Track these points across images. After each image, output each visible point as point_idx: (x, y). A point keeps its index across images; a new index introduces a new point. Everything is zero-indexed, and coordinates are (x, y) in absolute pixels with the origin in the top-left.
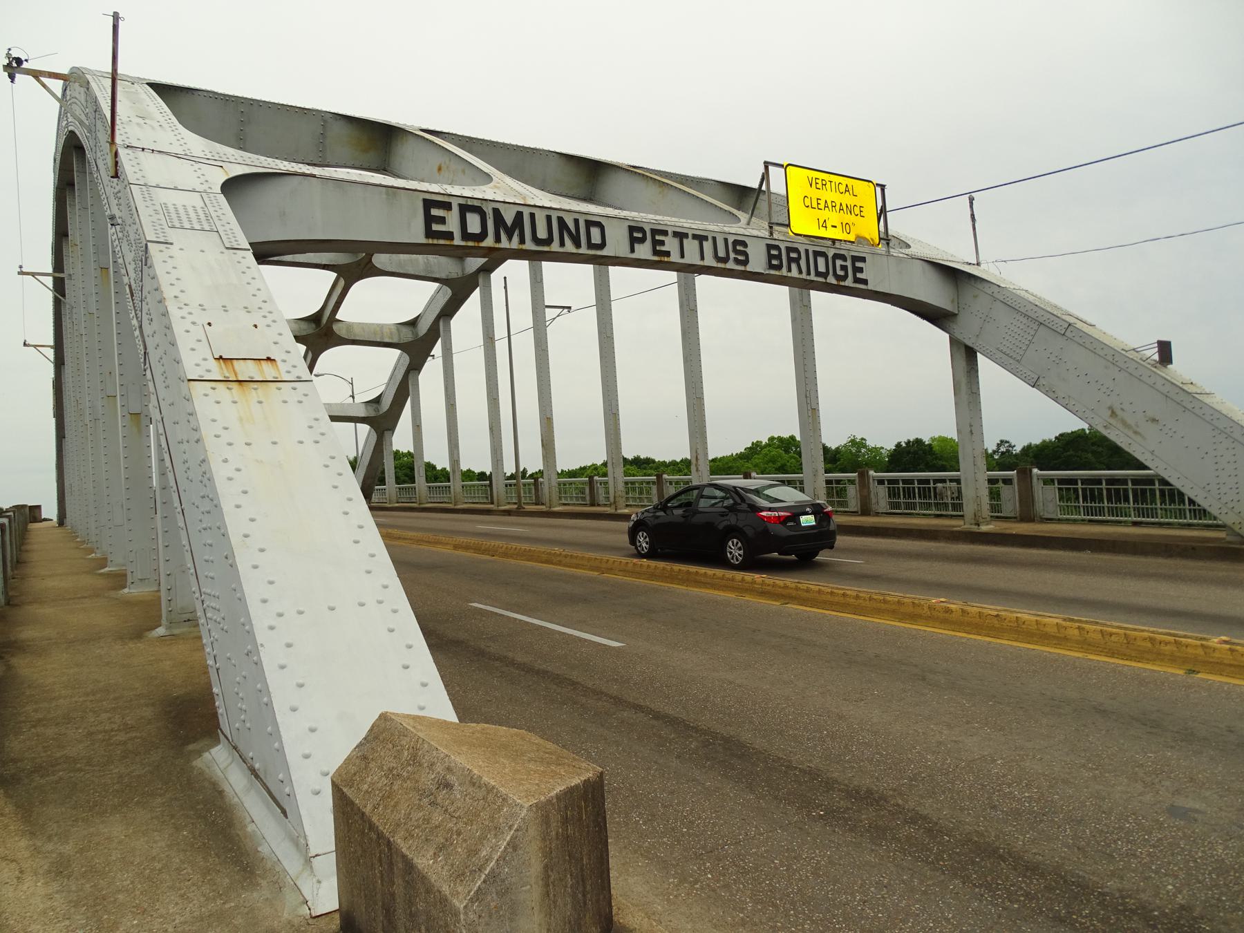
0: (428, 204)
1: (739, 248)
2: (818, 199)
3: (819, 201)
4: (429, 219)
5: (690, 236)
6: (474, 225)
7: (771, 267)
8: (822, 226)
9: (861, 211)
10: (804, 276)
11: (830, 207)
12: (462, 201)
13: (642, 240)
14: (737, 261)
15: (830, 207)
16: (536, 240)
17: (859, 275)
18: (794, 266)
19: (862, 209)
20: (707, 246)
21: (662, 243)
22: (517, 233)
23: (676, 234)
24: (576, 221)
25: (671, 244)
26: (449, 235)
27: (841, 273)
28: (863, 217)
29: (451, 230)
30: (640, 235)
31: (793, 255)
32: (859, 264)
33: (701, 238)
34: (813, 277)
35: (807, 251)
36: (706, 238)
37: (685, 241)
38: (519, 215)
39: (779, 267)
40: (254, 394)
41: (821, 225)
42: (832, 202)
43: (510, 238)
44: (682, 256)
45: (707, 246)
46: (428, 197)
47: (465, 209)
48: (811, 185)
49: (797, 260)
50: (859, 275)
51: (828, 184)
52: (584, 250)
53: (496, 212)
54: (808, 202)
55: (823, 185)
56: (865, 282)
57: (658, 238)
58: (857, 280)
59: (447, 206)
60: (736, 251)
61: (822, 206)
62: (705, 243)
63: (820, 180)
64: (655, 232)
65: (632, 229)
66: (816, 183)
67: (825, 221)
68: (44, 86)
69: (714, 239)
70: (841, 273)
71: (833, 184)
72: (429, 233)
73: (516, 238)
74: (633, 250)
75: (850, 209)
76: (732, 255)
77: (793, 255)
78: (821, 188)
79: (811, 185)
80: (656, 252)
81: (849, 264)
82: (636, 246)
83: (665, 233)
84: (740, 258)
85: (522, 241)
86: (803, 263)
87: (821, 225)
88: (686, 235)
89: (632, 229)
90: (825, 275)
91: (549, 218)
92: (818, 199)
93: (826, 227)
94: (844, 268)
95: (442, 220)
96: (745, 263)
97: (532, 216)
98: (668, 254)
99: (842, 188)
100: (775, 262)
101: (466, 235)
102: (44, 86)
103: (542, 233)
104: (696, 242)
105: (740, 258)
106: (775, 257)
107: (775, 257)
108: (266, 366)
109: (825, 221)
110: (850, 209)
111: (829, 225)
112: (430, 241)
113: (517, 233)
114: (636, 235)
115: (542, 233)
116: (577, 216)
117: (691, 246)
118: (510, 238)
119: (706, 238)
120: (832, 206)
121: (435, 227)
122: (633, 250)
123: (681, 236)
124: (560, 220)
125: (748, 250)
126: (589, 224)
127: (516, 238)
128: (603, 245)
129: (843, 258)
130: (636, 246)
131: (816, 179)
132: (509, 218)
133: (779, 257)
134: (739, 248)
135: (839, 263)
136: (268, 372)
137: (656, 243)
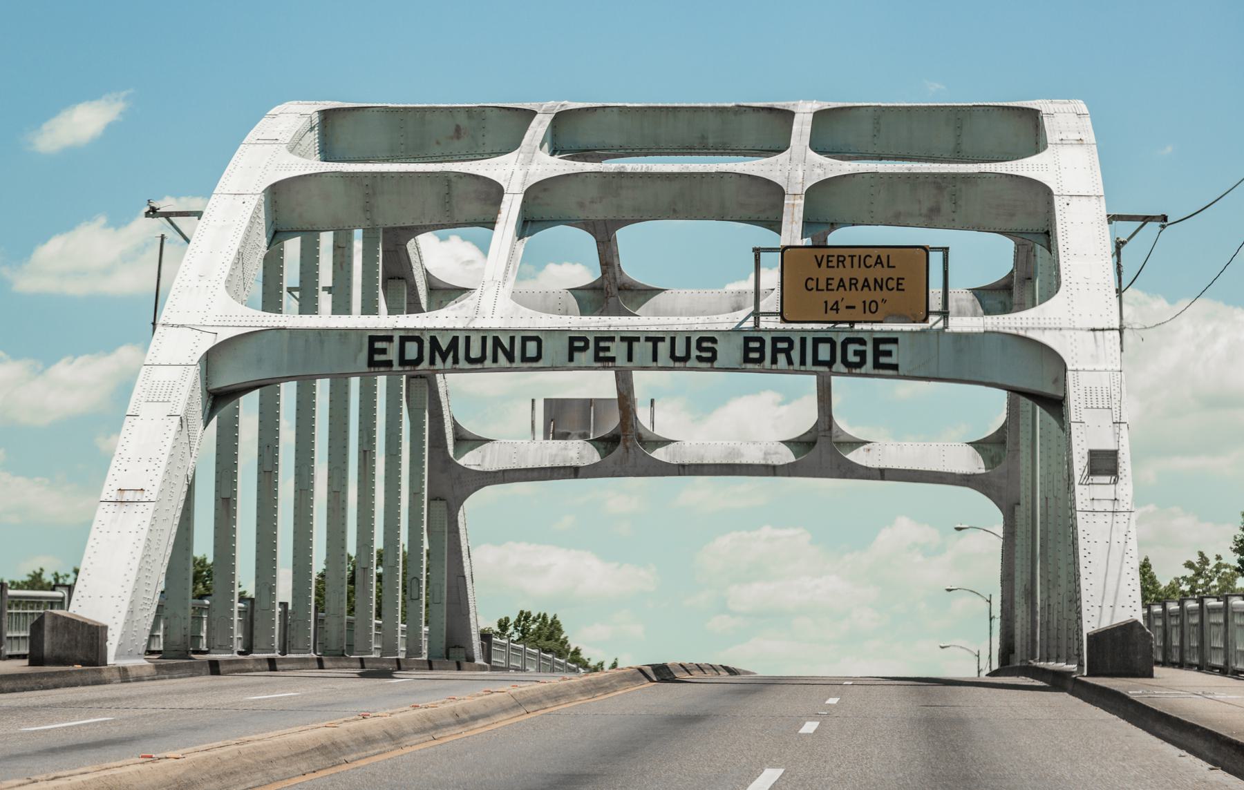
0: (373, 339)
1: (705, 345)
2: (828, 279)
3: (830, 282)
4: (372, 351)
5: (642, 339)
6: (411, 350)
7: (747, 360)
8: (831, 309)
9: (898, 284)
11: (847, 287)
12: (403, 334)
14: (700, 359)
15: (847, 287)
16: (469, 359)
17: (883, 360)
18: (782, 358)
19: (900, 281)
20: (663, 348)
21: (608, 349)
22: (451, 354)
24: (512, 339)
25: (617, 350)
26: (389, 364)
27: (852, 358)
28: (903, 290)
29: (391, 359)
30: (582, 344)
31: (781, 345)
33: (655, 340)
35: (803, 340)
36: (662, 339)
37: (635, 345)
38: (455, 339)
39: (761, 360)
40: (124, 508)
41: (829, 306)
42: (851, 279)
43: (444, 360)
44: (630, 359)
45: (663, 348)
47: (403, 340)
48: (819, 265)
49: (787, 352)
50: (883, 360)
53: (434, 340)
54: (811, 284)
55: (838, 261)
56: (895, 367)
57: (602, 344)
58: (877, 365)
59: (389, 339)
60: (699, 348)
61: (834, 286)
62: (660, 345)
64: (598, 340)
65: (572, 340)
66: (828, 261)
67: (837, 303)
68: (172, 223)
69: (673, 340)
70: (852, 358)
71: (856, 260)
72: (371, 363)
73: (450, 359)
74: (571, 359)
75: (879, 284)
76: (694, 352)
77: (781, 345)
78: (836, 266)
79: (819, 265)
80: (597, 359)
81: (869, 349)
82: (577, 355)
83: (612, 339)
84: (705, 355)
85: (456, 361)
86: (796, 354)
87: (829, 307)
88: (638, 339)
89: (572, 340)
90: (829, 364)
91: (484, 339)
92: (828, 279)
93: (837, 310)
94: (862, 354)
95: (384, 351)
96: (712, 359)
97: (468, 339)
98: (613, 359)
99: (870, 261)
101: (403, 362)
102: (172, 223)
103: (475, 352)
104: (650, 344)
105: (705, 355)
106: (754, 350)
107: (754, 350)
108: (139, 493)
109: (837, 303)
110: (879, 284)
111: (842, 306)
112: (372, 369)
113: (451, 354)
114: (577, 344)
115: (475, 352)
117: (642, 350)
118: (444, 360)
119: (662, 339)
120: (851, 284)
121: (377, 358)
122: (571, 359)
123: (630, 340)
124: (496, 340)
126: (525, 340)
127: (450, 359)
128: (538, 358)
129: (862, 342)
130: (577, 355)
131: (828, 256)
132: (444, 343)
133: (761, 350)
134: (705, 345)
135: (852, 348)
136: (138, 496)
137: (598, 349)
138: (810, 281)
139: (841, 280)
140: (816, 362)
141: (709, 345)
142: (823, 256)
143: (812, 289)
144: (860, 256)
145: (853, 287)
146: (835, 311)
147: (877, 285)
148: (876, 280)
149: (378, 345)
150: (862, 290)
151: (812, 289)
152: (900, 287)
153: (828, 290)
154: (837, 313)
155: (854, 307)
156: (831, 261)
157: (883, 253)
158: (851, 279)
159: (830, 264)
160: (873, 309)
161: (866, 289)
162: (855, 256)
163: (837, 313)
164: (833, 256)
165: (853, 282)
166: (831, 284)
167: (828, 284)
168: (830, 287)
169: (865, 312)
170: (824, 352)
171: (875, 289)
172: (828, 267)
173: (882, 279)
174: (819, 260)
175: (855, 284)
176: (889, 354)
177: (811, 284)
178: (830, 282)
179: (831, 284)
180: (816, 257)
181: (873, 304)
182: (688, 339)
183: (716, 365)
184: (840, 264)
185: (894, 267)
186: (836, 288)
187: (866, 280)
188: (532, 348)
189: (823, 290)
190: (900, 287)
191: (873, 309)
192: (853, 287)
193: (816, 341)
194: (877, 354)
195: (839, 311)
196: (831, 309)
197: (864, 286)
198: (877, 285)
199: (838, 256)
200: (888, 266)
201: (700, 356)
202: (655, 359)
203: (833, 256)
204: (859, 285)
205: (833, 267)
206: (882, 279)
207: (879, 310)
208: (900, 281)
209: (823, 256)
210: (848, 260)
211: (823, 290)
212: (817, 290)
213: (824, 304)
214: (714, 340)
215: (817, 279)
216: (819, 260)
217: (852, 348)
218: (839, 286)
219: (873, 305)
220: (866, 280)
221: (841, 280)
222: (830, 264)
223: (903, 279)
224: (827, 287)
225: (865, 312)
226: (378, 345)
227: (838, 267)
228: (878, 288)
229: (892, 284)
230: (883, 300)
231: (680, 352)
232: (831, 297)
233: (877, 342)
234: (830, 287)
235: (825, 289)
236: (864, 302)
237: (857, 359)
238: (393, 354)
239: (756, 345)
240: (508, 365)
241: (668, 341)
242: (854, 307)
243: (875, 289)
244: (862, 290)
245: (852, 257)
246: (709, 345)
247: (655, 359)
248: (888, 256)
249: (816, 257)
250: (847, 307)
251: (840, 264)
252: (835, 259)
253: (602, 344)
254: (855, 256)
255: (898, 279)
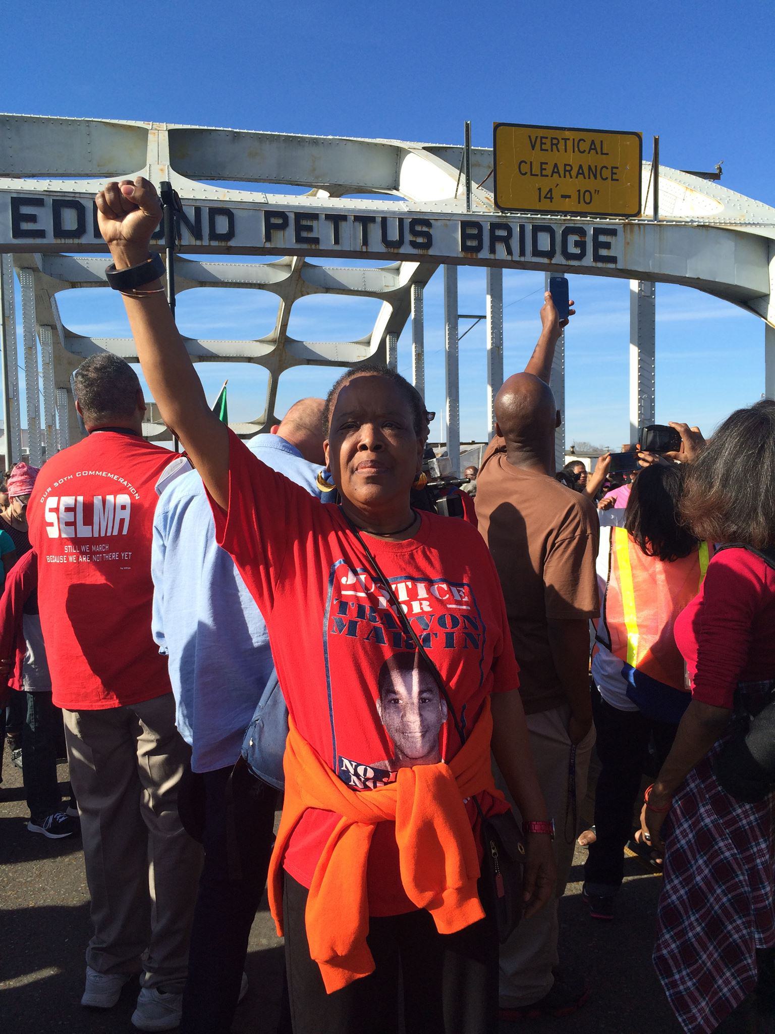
0: (19, 201)
2: (542, 163)
3: (544, 166)
4: (17, 218)
8: (545, 198)
9: (613, 173)
10: (516, 257)
11: (562, 173)
13: (284, 226)
14: (414, 244)
15: (562, 173)
17: (603, 252)
19: (615, 170)
20: (375, 232)
23: (329, 217)
26: (41, 234)
27: (572, 249)
28: (617, 180)
30: (280, 221)
31: (502, 233)
32: (602, 238)
34: (529, 258)
35: (522, 228)
37: (343, 225)
39: (479, 248)
41: (543, 195)
42: (565, 165)
44: (337, 241)
45: (375, 232)
46: (15, 195)
49: (506, 240)
50: (603, 252)
51: (562, 142)
52: (206, 242)
54: (525, 168)
55: (552, 144)
56: (613, 260)
57: (304, 223)
58: (597, 258)
61: (548, 172)
63: (549, 139)
66: (542, 143)
67: (551, 190)
69: (384, 220)
70: (572, 249)
71: (570, 143)
72: (18, 232)
75: (594, 172)
76: (408, 237)
78: (550, 150)
80: (299, 239)
83: (314, 216)
84: (420, 240)
87: (543, 195)
88: (344, 218)
90: (550, 254)
92: (542, 163)
93: (551, 198)
94: (581, 244)
95: (33, 218)
96: (428, 245)
98: (316, 241)
99: (585, 146)
100: (469, 243)
101: (59, 232)
105: (420, 240)
106: (472, 237)
107: (472, 237)
109: (551, 190)
110: (594, 172)
111: (556, 194)
114: (274, 221)
116: (198, 204)
119: (372, 219)
120: (565, 170)
121: (25, 226)
122: (268, 238)
125: (431, 231)
128: (230, 235)
131: (542, 138)
133: (479, 237)
135: (572, 239)
137: (299, 228)
138: (523, 164)
139: (556, 165)
140: (536, 253)
141: (425, 229)
142: (537, 137)
143: (526, 173)
144: (573, 139)
145: (567, 173)
146: (549, 200)
147: (591, 173)
148: (590, 167)
149: (25, 210)
150: (577, 177)
151: (526, 173)
152: (615, 177)
153: (542, 175)
154: (551, 202)
155: (569, 197)
156: (545, 144)
157: (598, 138)
158: (565, 165)
159: (544, 147)
160: (588, 200)
161: (580, 176)
162: (569, 139)
163: (551, 202)
164: (547, 138)
165: (568, 168)
166: (545, 169)
167: (542, 169)
168: (544, 173)
169: (579, 203)
170: (544, 242)
171: (589, 178)
172: (542, 150)
173: (596, 166)
174: (533, 142)
175: (569, 171)
176: (607, 246)
177: (525, 168)
178: (544, 166)
179: (545, 169)
180: (530, 137)
181: (587, 195)
182: (401, 221)
183: (431, 252)
184: (554, 147)
185: (607, 154)
186: (550, 176)
187: (581, 167)
188: (222, 226)
189: (537, 175)
190: (615, 177)
191: (588, 200)
192: (567, 173)
193: (537, 229)
194: (598, 245)
195: (553, 200)
196: (545, 198)
197: (578, 173)
198: (594, 172)
199: (552, 139)
200: (602, 154)
201: (415, 241)
202: (365, 242)
203: (547, 138)
204: (574, 173)
205: (547, 150)
206: (596, 166)
207: (592, 201)
208: (615, 170)
209: (537, 137)
210: (561, 146)
211: (537, 175)
212: (532, 175)
213: (538, 191)
214: (426, 222)
215: (531, 162)
216: (533, 142)
217: (572, 239)
218: (553, 172)
219: (587, 195)
220: (581, 167)
221: (556, 165)
222: (544, 147)
223: (617, 168)
224: (541, 173)
225: (579, 203)
226: (25, 210)
227: (552, 151)
228: (591, 175)
229: (607, 173)
230: (596, 190)
231: (394, 235)
232: (546, 184)
233: (598, 231)
234: (544, 173)
235: (539, 173)
236: (579, 191)
237: (577, 251)
238: (46, 221)
239: (475, 232)
240: (194, 242)
241: (379, 220)
242: (569, 197)
243: (589, 178)
244: (577, 177)
245: (566, 140)
246: (425, 229)
247: (365, 242)
248: (602, 142)
249: (530, 137)
250: (563, 196)
251: (554, 147)
252: (548, 142)
253: (304, 223)
254: (569, 139)
255: (613, 168)
